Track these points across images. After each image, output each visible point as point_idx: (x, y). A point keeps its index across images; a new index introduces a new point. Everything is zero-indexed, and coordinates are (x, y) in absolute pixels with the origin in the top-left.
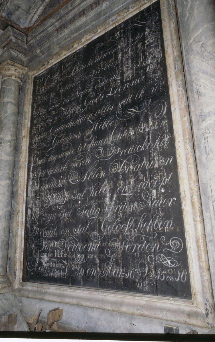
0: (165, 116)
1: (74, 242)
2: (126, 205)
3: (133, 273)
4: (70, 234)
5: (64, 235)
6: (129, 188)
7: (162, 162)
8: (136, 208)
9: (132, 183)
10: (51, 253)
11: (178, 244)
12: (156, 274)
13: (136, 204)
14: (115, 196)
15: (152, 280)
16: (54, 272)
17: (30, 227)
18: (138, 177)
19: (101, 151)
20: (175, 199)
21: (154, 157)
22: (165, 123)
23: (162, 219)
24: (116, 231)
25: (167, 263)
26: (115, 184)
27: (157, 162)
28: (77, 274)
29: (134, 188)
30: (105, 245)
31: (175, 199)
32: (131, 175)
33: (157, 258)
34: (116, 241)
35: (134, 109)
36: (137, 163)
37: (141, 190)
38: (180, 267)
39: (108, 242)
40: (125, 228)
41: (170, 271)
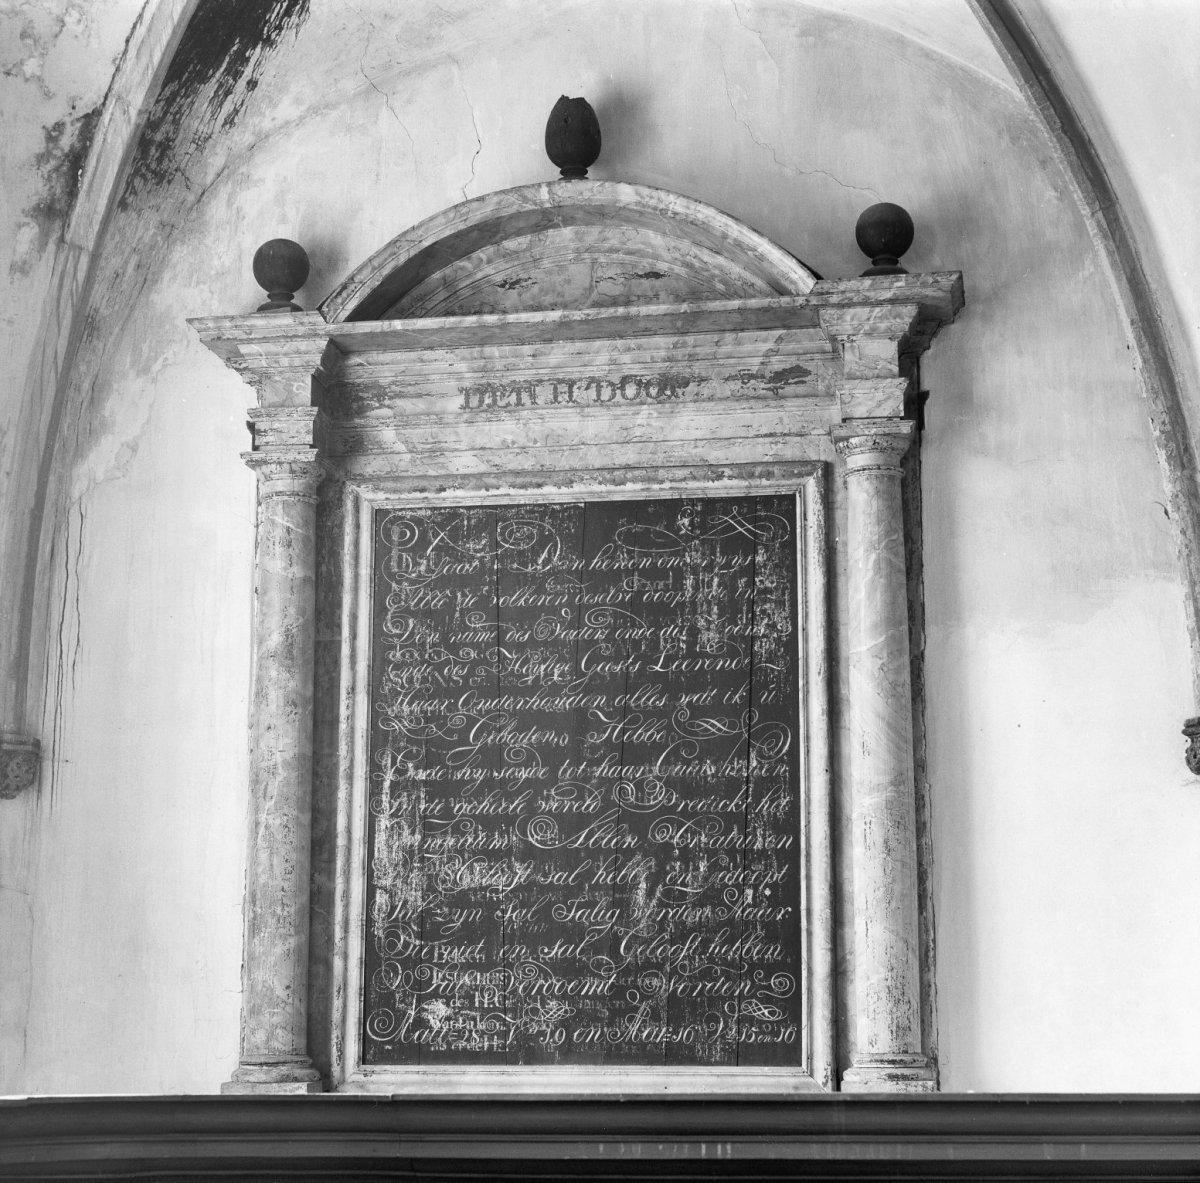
3: (689, 1033)
4: (527, 958)
5: (508, 957)
6: (693, 876)
7: (771, 842)
8: (707, 917)
9: (702, 870)
12: (739, 1033)
13: (708, 911)
15: (729, 1044)
16: (468, 1040)
20: (790, 909)
21: (755, 828)
22: (785, 771)
23: (761, 941)
25: (763, 1014)
26: (661, 866)
27: (760, 839)
29: (706, 879)
31: (790, 909)
33: (743, 1006)
38: (785, 1020)
40: (679, 951)
41: (767, 1027)
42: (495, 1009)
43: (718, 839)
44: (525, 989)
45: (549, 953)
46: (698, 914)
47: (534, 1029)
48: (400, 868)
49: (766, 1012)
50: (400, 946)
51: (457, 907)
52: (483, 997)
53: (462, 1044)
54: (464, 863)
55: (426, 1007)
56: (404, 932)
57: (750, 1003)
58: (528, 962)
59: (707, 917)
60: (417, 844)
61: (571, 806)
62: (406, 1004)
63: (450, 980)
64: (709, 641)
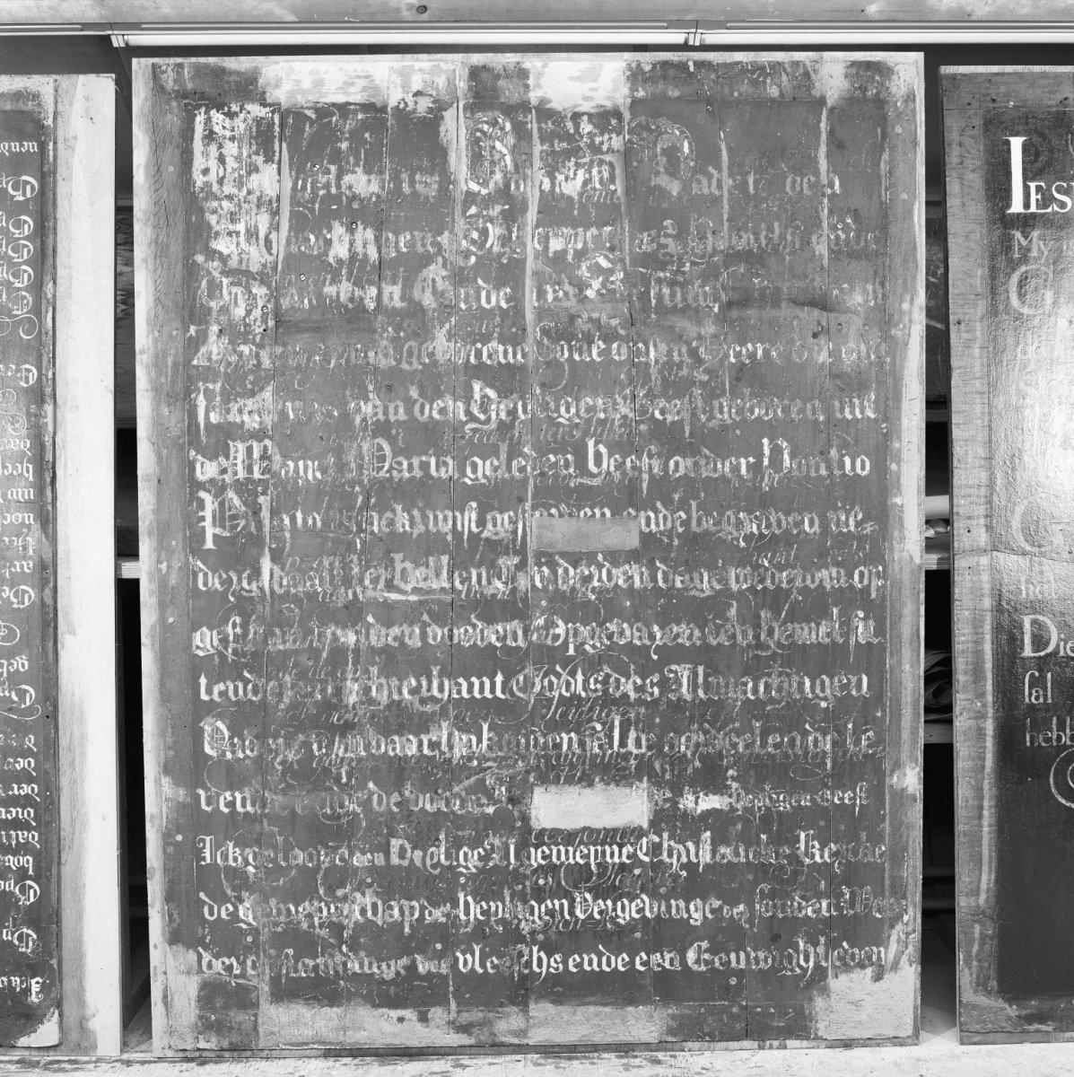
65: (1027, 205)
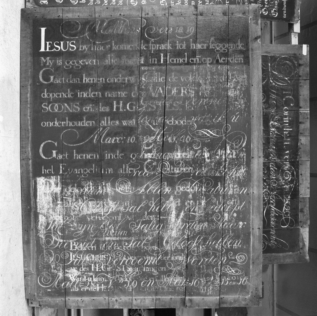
0: (244, 149)
1: (123, 256)
2: (195, 223)
3: (197, 282)
4: (117, 248)
5: (108, 248)
6: (199, 208)
7: (236, 191)
9: (203, 204)
10: (84, 267)
11: (243, 258)
12: (221, 281)
13: (206, 224)
14: (182, 214)
15: (216, 287)
16: (89, 286)
17: (46, 238)
18: (211, 199)
19: (166, 165)
20: (246, 223)
21: (229, 184)
22: (244, 156)
23: (232, 238)
24: (181, 247)
25: (232, 272)
26: (183, 203)
27: (232, 189)
28: (127, 286)
29: (205, 209)
30: (167, 258)
31: (246, 223)
32: (203, 197)
33: (223, 268)
34: (181, 255)
35: (211, 131)
36: (211, 185)
37: (212, 212)
38: (242, 275)
39: (171, 256)
40: (192, 244)
41: (234, 278)
42: (102, 272)
43: (211, 190)
44: (116, 262)
45: (128, 245)
46: (201, 226)
47: (122, 280)
48: (51, 204)
49: (233, 271)
50: (52, 242)
51: (81, 223)
52: (96, 266)
53: (86, 288)
54: (83, 202)
55: (68, 271)
56: (54, 235)
57: (226, 267)
58: (117, 250)
59: (205, 227)
60: (59, 192)
61: (137, 173)
62: (57, 270)
63: (79, 259)
64: (206, 89)
65: (46, 49)
